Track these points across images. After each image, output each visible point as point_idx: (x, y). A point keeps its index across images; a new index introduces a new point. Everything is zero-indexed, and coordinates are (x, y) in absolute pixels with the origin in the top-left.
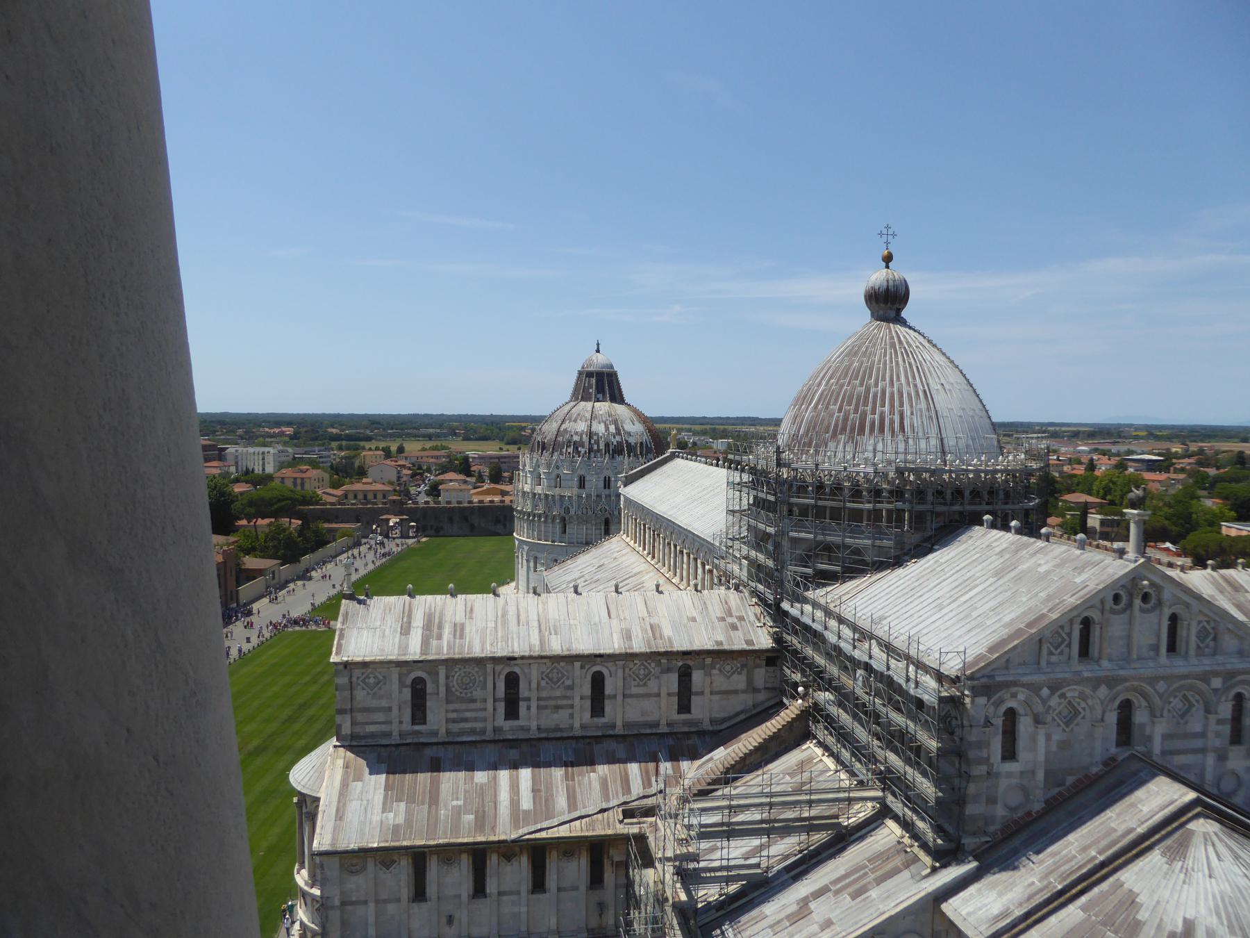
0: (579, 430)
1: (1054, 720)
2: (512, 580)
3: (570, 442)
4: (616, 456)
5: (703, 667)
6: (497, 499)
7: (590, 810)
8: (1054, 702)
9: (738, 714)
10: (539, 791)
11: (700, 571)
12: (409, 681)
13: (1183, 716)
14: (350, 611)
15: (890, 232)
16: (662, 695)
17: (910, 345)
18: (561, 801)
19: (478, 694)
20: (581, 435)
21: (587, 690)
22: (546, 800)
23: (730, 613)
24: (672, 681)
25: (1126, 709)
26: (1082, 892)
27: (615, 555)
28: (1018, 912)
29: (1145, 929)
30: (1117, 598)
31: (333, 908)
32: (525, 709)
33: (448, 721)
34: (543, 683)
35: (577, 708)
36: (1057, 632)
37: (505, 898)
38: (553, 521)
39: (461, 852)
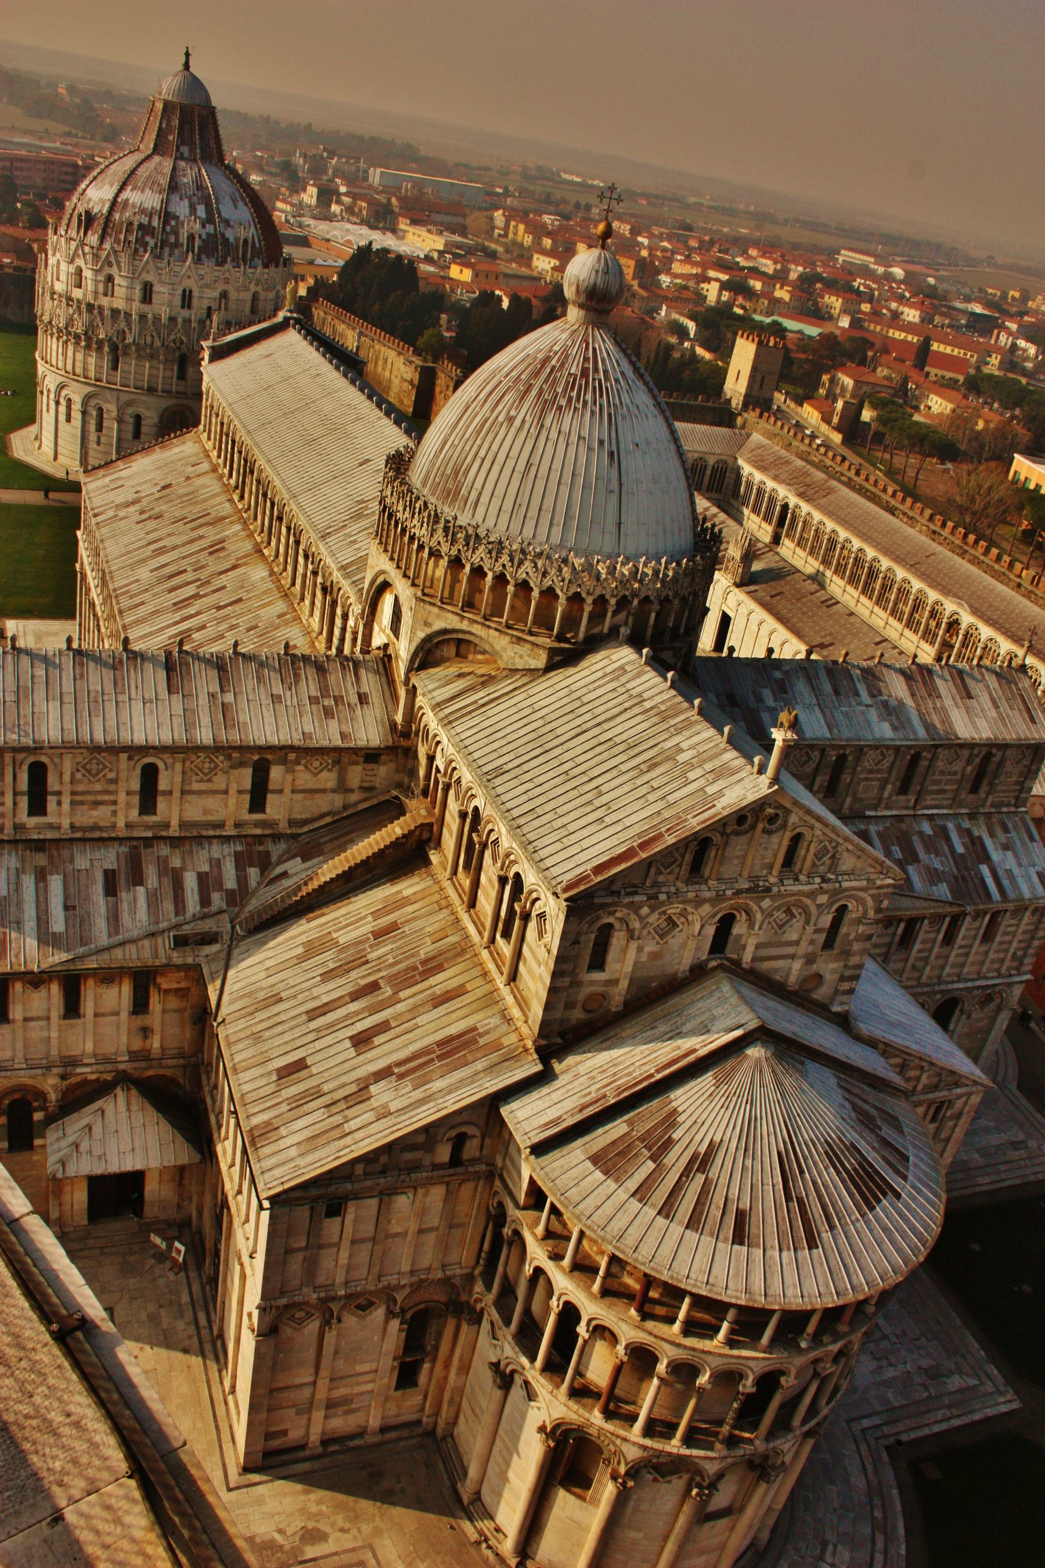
0: (148, 205)
1: (649, 933)
3: (130, 224)
4: (203, 256)
5: (284, 761)
7: (135, 934)
8: (652, 919)
9: (323, 816)
10: (74, 908)
11: (301, 560)
15: (615, 196)
16: (231, 792)
17: (607, 379)
21: (136, 785)
25: (726, 923)
29: (677, 1150)
32: (54, 804)
37: (32, 1024)
38: (100, 349)
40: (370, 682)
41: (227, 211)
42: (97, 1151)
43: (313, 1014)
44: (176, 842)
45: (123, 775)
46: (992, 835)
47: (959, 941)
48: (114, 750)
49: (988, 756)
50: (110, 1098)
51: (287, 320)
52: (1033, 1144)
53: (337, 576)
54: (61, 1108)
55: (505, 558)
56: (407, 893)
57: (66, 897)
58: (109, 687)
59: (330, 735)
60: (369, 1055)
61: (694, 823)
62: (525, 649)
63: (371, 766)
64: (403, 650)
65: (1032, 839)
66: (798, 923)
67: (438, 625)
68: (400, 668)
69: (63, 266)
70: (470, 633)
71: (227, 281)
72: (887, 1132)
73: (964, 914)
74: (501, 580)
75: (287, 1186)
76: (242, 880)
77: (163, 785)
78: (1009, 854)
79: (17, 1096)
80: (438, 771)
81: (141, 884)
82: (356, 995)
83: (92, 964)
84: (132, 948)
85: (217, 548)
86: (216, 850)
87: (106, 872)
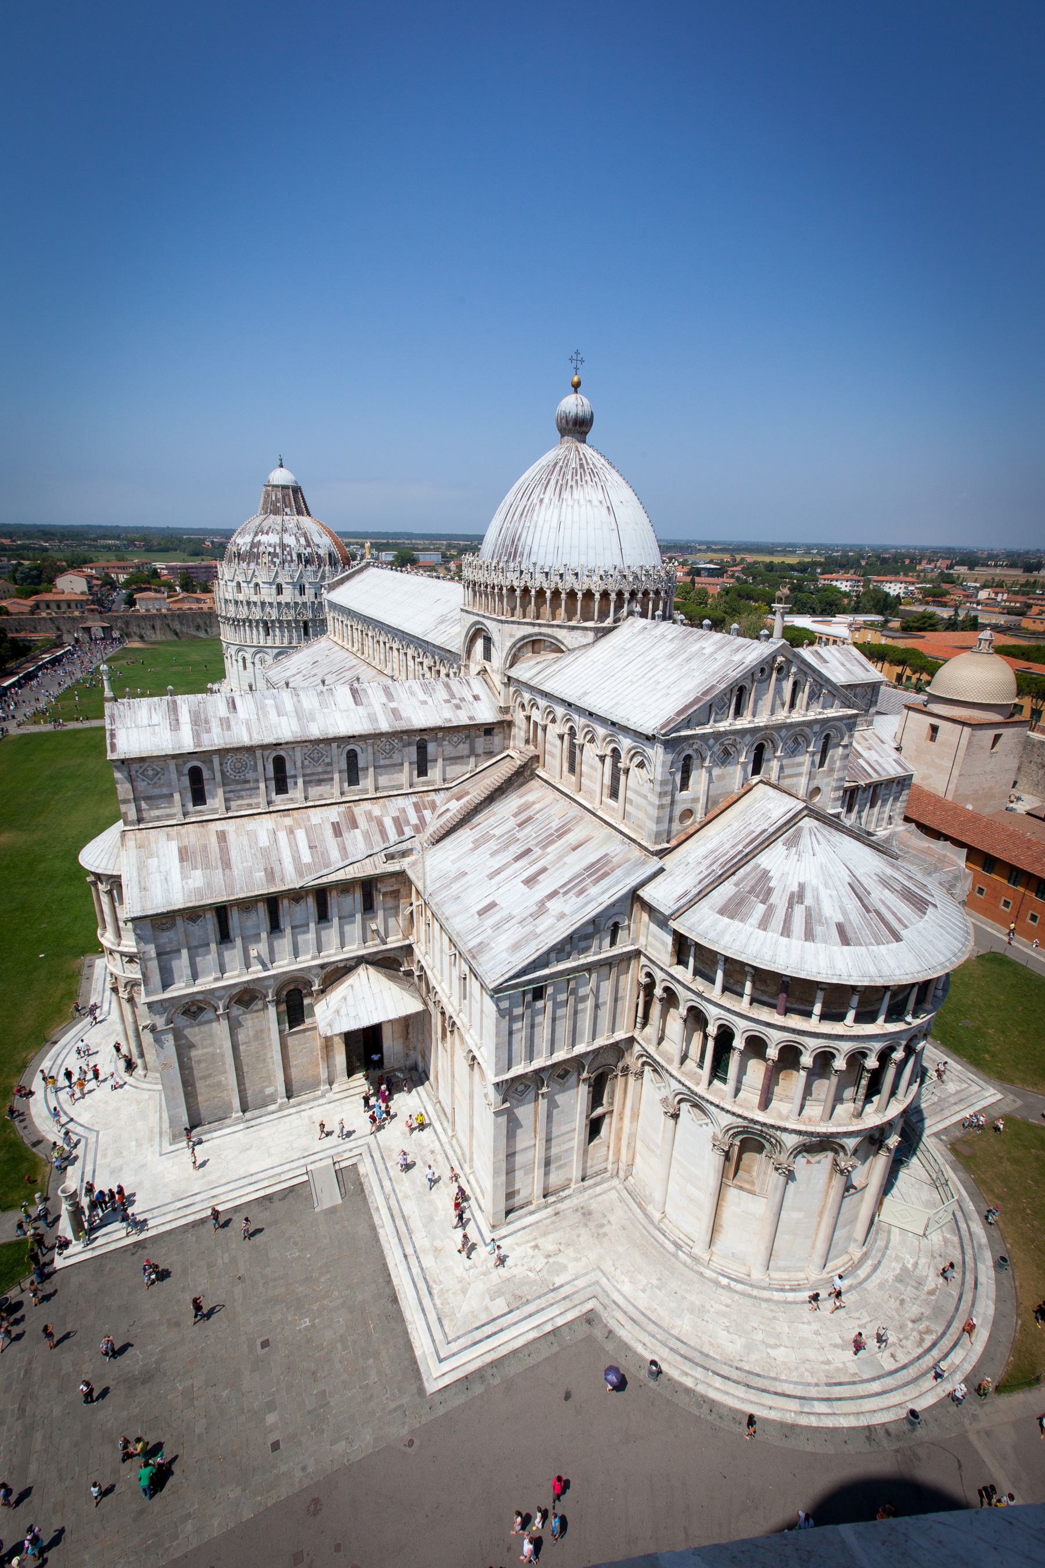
0: (272, 542)
5: (436, 740)
6: (194, 606)
8: (715, 749)
11: (411, 663)
12: (186, 771)
14: (116, 712)
17: (596, 467)
18: (335, 854)
19: (250, 775)
21: (344, 765)
22: (323, 853)
23: (453, 696)
24: (412, 752)
26: (733, 873)
27: (327, 652)
28: (695, 891)
29: (775, 892)
30: (762, 670)
31: (151, 959)
36: (722, 699)
38: (257, 627)
39: (257, 901)
41: (316, 539)
42: (352, 1014)
43: (491, 876)
45: (335, 759)
48: (328, 741)
57: (309, 841)
58: (317, 705)
59: (462, 718)
60: (538, 887)
61: (734, 675)
62: (578, 633)
63: (488, 738)
69: (229, 583)
70: (540, 634)
74: (556, 593)
75: (506, 977)
78: (873, 752)
79: (292, 987)
80: (536, 724)
82: (517, 858)
86: (401, 802)
87: (333, 823)
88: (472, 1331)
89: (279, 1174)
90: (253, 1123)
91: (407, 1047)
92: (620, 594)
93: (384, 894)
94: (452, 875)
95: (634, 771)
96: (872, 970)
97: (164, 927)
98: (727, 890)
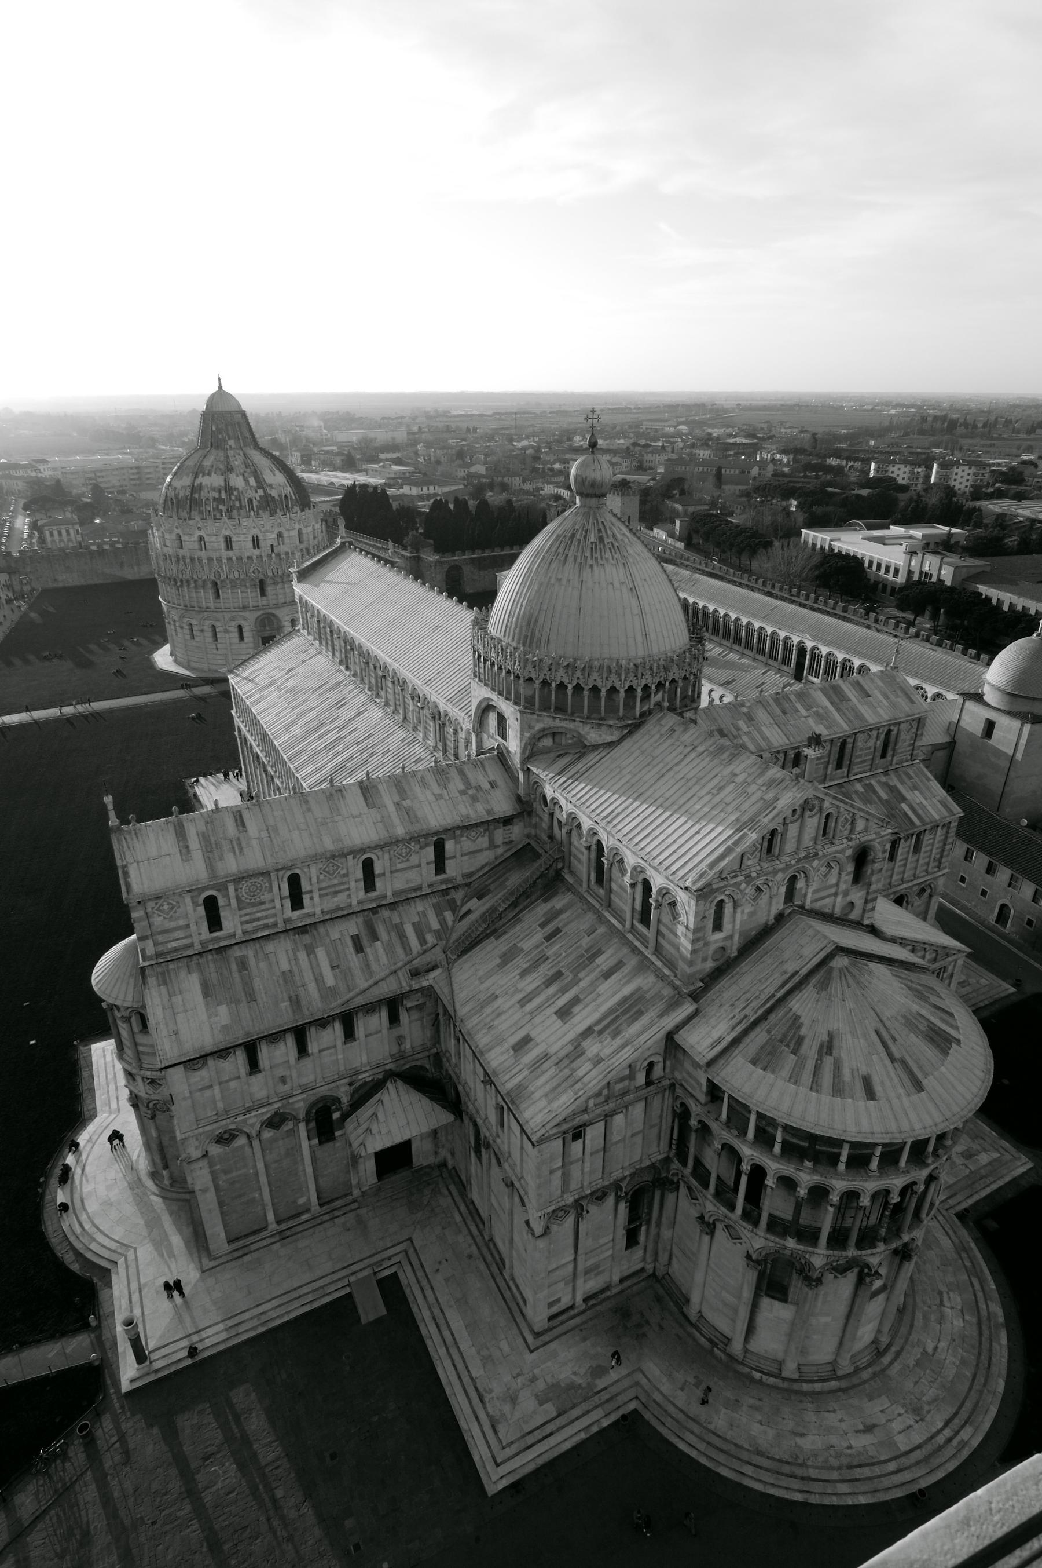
0: (216, 484)
2: (165, 641)
5: (454, 838)
7: (382, 975)
8: (747, 891)
9: (483, 867)
12: (201, 901)
13: (825, 876)
19: (266, 897)
20: (220, 492)
21: (360, 874)
24: (430, 853)
25: (793, 879)
29: (807, 1042)
30: (795, 811)
33: (242, 923)
34: (322, 877)
35: (353, 890)
37: (325, 1053)
40: (494, 773)
42: (384, 1130)
43: (523, 1002)
44: (393, 906)
45: (351, 870)
46: (902, 783)
47: (899, 857)
48: (344, 855)
49: (889, 731)
50: (384, 1091)
51: (343, 544)
52: (973, 981)
53: (443, 706)
54: (351, 1106)
55: (578, 674)
56: (558, 906)
57: (331, 961)
59: (478, 812)
63: (507, 828)
64: (514, 745)
65: (928, 780)
66: (835, 871)
67: (538, 726)
68: (516, 760)
69: (167, 536)
71: (280, 525)
72: (933, 999)
73: (900, 839)
74: (578, 688)
76: (443, 922)
77: (378, 869)
78: (916, 792)
79: (320, 1105)
80: (560, 822)
81: (378, 940)
83: (360, 1001)
84: (382, 984)
85: (340, 704)
86: (420, 906)
88: (523, 1436)
89: (322, 1287)
90: (288, 1233)
91: (437, 1146)
92: (646, 687)
93: (410, 1008)
94: (483, 997)
95: (666, 909)
96: (893, 1127)
97: (196, 1067)
98: (758, 1038)
